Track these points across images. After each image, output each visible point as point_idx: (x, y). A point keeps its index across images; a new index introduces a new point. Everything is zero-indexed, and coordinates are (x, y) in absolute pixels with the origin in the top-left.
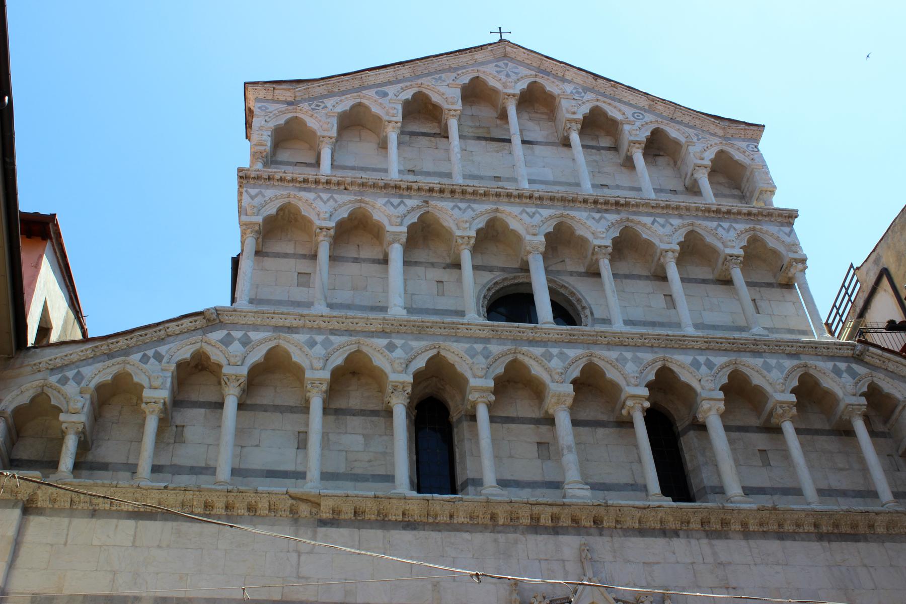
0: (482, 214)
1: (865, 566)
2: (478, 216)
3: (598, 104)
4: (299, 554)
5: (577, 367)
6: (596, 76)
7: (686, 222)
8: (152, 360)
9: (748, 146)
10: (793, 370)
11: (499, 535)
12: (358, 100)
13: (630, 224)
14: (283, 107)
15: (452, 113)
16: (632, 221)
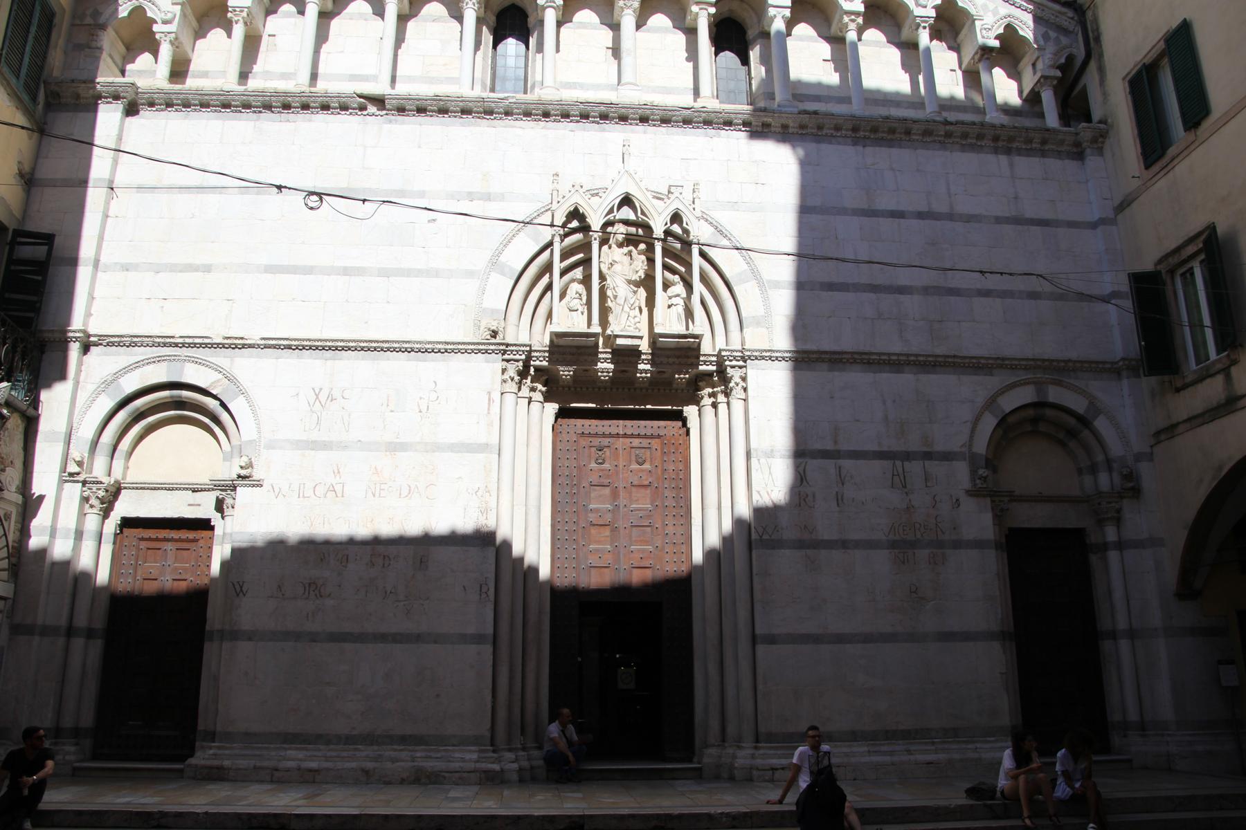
1: (892, 169)
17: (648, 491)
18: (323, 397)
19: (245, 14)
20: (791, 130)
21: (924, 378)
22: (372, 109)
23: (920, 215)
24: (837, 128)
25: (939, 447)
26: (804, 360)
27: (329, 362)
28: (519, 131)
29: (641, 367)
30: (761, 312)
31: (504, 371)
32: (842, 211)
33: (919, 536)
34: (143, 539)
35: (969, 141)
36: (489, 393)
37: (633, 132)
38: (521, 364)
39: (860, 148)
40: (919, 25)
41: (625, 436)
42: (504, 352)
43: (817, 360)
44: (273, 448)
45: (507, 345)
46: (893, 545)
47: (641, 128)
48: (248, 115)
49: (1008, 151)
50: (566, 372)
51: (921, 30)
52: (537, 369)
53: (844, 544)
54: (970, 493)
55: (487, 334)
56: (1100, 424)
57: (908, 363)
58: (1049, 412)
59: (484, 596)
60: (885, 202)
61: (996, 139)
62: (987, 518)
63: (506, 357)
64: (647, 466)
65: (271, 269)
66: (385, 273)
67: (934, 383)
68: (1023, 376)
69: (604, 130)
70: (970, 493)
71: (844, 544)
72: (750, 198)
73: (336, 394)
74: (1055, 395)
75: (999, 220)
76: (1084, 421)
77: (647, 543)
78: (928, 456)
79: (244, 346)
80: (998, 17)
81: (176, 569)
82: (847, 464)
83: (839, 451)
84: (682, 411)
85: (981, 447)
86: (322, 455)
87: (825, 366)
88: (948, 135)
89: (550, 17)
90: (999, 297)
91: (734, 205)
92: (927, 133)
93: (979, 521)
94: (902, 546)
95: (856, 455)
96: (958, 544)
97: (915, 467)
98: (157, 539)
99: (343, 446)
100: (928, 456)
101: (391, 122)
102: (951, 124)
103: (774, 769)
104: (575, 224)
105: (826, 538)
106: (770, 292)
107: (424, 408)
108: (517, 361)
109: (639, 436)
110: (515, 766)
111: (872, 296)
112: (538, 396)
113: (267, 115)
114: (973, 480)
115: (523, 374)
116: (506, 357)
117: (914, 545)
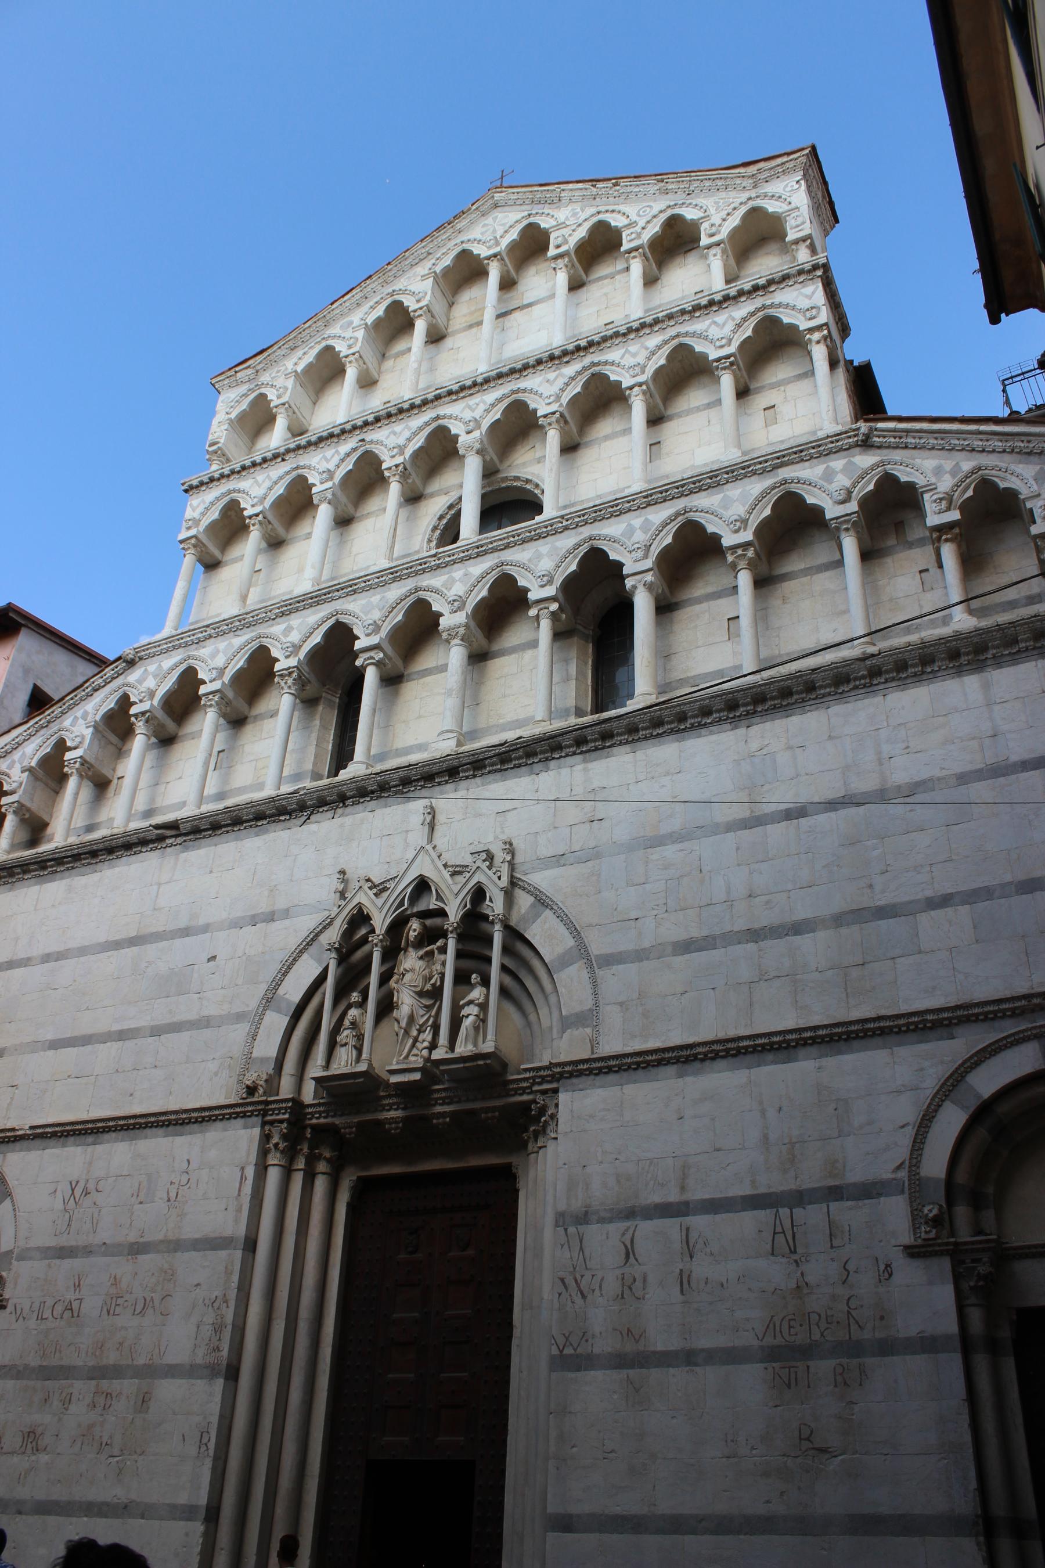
0: (421, 429)
1: (790, 748)
3: (601, 217)
4: (159, 885)
5: (484, 586)
6: (594, 181)
7: (667, 337)
8: (81, 721)
10: (764, 494)
12: (324, 344)
13: (596, 369)
14: (243, 389)
15: (417, 314)
16: (598, 364)
18: (78, 1192)
19: (77, 765)
21: (831, 1062)
25: (855, 1175)
27: (90, 1149)
29: (439, 1109)
31: (266, 1137)
33: (816, 1336)
35: (911, 670)
36: (243, 1169)
38: (285, 1125)
40: (838, 529)
42: (264, 1116)
43: (660, 1063)
45: (267, 1103)
46: (772, 1355)
51: (843, 535)
53: (689, 1358)
54: (913, 1252)
57: (804, 1043)
59: (204, 1448)
62: (945, 1294)
63: (269, 1118)
64: (470, 1252)
65: (55, 1045)
66: (157, 1031)
68: (1009, 1027)
70: (913, 1252)
71: (689, 1358)
73: (91, 1186)
75: (963, 779)
78: (835, 1193)
82: (699, 1222)
83: (687, 1204)
85: (935, 1164)
86: (68, 1263)
87: (671, 1070)
89: (371, 677)
90: (964, 903)
91: (558, 860)
93: (928, 1300)
94: (787, 1356)
95: (714, 1206)
96: (887, 1347)
97: (813, 1216)
99: (88, 1251)
100: (835, 1193)
102: (873, 655)
104: (363, 931)
105: (660, 1347)
106: (600, 973)
107: (173, 1195)
111: (751, 947)
112: (322, 1166)
114: (915, 1228)
117: (806, 1352)
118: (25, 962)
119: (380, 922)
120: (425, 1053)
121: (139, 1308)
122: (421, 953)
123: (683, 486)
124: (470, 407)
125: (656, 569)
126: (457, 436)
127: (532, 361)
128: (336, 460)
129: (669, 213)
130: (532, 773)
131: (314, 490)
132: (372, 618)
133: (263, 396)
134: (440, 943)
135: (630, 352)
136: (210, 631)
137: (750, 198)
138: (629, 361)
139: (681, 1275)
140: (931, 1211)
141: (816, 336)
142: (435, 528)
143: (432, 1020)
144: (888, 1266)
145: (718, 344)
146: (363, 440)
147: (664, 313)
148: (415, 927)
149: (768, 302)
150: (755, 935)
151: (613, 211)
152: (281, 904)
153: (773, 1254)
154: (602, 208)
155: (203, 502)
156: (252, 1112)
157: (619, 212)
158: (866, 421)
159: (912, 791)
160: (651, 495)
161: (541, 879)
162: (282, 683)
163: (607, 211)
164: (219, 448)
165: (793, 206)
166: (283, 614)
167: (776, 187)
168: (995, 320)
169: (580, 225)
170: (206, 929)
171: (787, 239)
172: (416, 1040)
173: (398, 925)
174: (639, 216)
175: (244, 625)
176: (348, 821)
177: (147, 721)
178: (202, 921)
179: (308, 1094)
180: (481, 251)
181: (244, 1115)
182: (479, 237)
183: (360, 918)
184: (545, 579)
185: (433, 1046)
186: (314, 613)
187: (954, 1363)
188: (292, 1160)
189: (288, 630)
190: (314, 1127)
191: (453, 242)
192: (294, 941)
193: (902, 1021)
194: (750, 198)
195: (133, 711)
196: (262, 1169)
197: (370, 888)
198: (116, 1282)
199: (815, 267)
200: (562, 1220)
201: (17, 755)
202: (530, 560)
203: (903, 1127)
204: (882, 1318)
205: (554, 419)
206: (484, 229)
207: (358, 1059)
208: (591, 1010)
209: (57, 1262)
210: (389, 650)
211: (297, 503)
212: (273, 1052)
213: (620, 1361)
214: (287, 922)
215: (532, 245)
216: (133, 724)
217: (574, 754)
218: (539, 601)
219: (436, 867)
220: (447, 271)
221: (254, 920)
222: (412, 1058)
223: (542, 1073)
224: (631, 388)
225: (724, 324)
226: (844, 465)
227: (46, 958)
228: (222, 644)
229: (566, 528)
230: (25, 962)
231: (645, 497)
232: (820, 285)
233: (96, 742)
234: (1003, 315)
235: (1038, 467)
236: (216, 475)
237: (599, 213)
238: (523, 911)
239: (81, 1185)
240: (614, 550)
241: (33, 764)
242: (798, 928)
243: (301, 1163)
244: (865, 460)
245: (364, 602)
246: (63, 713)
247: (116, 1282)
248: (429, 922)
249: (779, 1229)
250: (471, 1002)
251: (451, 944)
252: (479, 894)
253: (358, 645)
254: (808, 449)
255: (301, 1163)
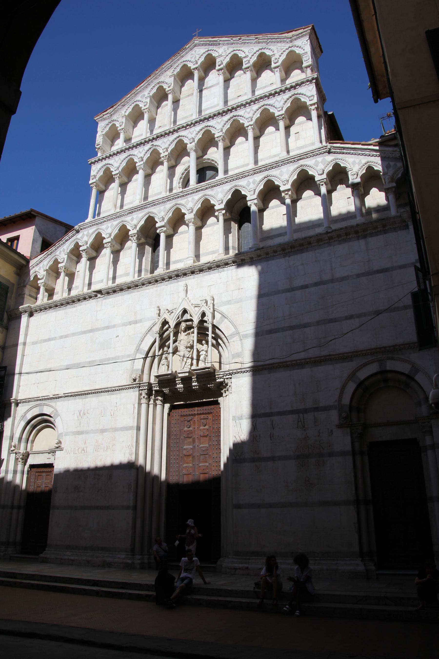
1: (303, 264)
2: (171, 143)
4: (97, 311)
8: (62, 252)
9: (303, 42)
11: (158, 288)
12: (135, 103)
14: (107, 122)
15: (169, 92)
17: (207, 438)
18: (82, 414)
19: (63, 269)
20: (254, 259)
22: (99, 295)
23: (316, 284)
24: (275, 252)
26: (258, 370)
27: (84, 400)
28: (147, 291)
29: (194, 384)
30: (240, 350)
32: (278, 292)
34: (37, 472)
36: (134, 405)
37: (189, 279)
38: (146, 390)
39: (287, 258)
41: (198, 414)
42: (139, 388)
44: (66, 435)
45: (140, 384)
47: (192, 276)
48: (63, 308)
49: (365, 237)
50: (166, 391)
52: (155, 391)
53: (273, 459)
55: (132, 381)
56: (419, 377)
58: (389, 375)
60: (299, 282)
61: (357, 232)
62: (348, 439)
63: (141, 388)
64: (207, 427)
67: (321, 371)
69: (178, 282)
70: (339, 426)
71: (273, 459)
72: (234, 298)
73: (86, 412)
74: (390, 365)
75: (358, 276)
76: (410, 377)
77: (206, 462)
78: (316, 409)
79: (59, 397)
80: (362, 165)
81: (46, 483)
83: (272, 413)
84: (218, 400)
85: (346, 400)
86: (81, 436)
88: (330, 238)
91: (229, 302)
92: (319, 241)
93: (343, 441)
98: (40, 472)
99: (87, 432)
100: (316, 409)
101: (105, 299)
102: (330, 233)
103: (236, 569)
107: (112, 414)
108: (145, 389)
109: (203, 414)
110: (139, 561)
112: (159, 402)
113: (69, 306)
115: (149, 394)
116: (141, 388)
118: (54, 339)
119: (172, 324)
120: (189, 366)
121: (105, 449)
122: (186, 333)
123: (266, 167)
124: (190, 133)
125: (258, 198)
126: (187, 144)
127: (212, 115)
128: (144, 153)
129: (260, 51)
130: (219, 272)
131: (137, 165)
132: (162, 215)
133: (114, 125)
134: (192, 330)
135: (247, 112)
136: (105, 219)
137: (289, 47)
138: (247, 116)
139: (271, 434)
140: (344, 415)
141: (313, 107)
142: (181, 178)
143: (191, 356)
144: (332, 431)
145: (278, 109)
146: (153, 145)
147: (259, 96)
148: (183, 325)
149: (296, 93)
150: (292, 328)
151: (239, 50)
152: (139, 318)
153: (298, 428)
154: (235, 49)
155: (97, 168)
156: (135, 387)
157: (242, 51)
158: (330, 143)
159: (342, 279)
160: (256, 170)
161: (223, 309)
162: (132, 239)
163: (237, 50)
164: (100, 146)
165: (305, 51)
166: (130, 213)
167: (299, 42)
168: (376, 101)
169: (227, 56)
170: (114, 326)
171: (303, 66)
172: (186, 362)
173: (178, 325)
174: (249, 53)
175: (116, 217)
176: (159, 289)
177: (86, 252)
178: (113, 324)
179: (153, 380)
180: (192, 66)
181: (133, 388)
182: (190, 59)
183: (165, 323)
184: (220, 201)
185: (192, 364)
186: (141, 213)
187: (349, 459)
188: (149, 401)
189: (132, 219)
190: (155, 390)
191: (180, 61)
192: (144, 330)
193: (337, 356)
194: (289, 47)
195: (81, 249)
196: (140, 404)
197: (168, 313)
198: (97, 441)
199: (313, 79)
200: (234, 418)
201: (41, 265)
202: (215, 194)
203: (336, 389)
204: (330, 446)
205: (220, 139)
206: (191, 56)
207: (168, 370)
208: (241, 352)
209: (78, 436)
210: (168, 227)
211: (130, 170)
212: (140, 367)
213: (253, 460)
214: (141, 324)
215: (209, 64)
216: (81, 254)
217: (233, 266)
218: (218, 210)
219: (189, 305)
220: (178, 74)
221: (130, 323)
222: (185, 368)
223: (226, 373)
224: (248, 127)
225: (280, 101)
226: (322, 160)
227: (61, 337)
228: (109, 224)
229: (227, 182)
230: (54, 339)
231: (254, 171)
232: (315, 86)
233: (69, 260)
234: (379, 100)
235: (387, 163)
236: (101, 158)
237: (234, 51)
238: (218, 319)
239: (82, 412)
240: (244, 190)
241: (47, 268)
242: (305, 326)
243: (152, 402)
244: (330, 158)
245: (158, 209)
246: (56, 249)
247: (97, 441)
248: (188, 323)
249: (299, 420)
250: (203, 350)
251: (196, 330)
252: (203, 315)
253: (157, 225)
254: (309, 153)
255: (152, 402)
